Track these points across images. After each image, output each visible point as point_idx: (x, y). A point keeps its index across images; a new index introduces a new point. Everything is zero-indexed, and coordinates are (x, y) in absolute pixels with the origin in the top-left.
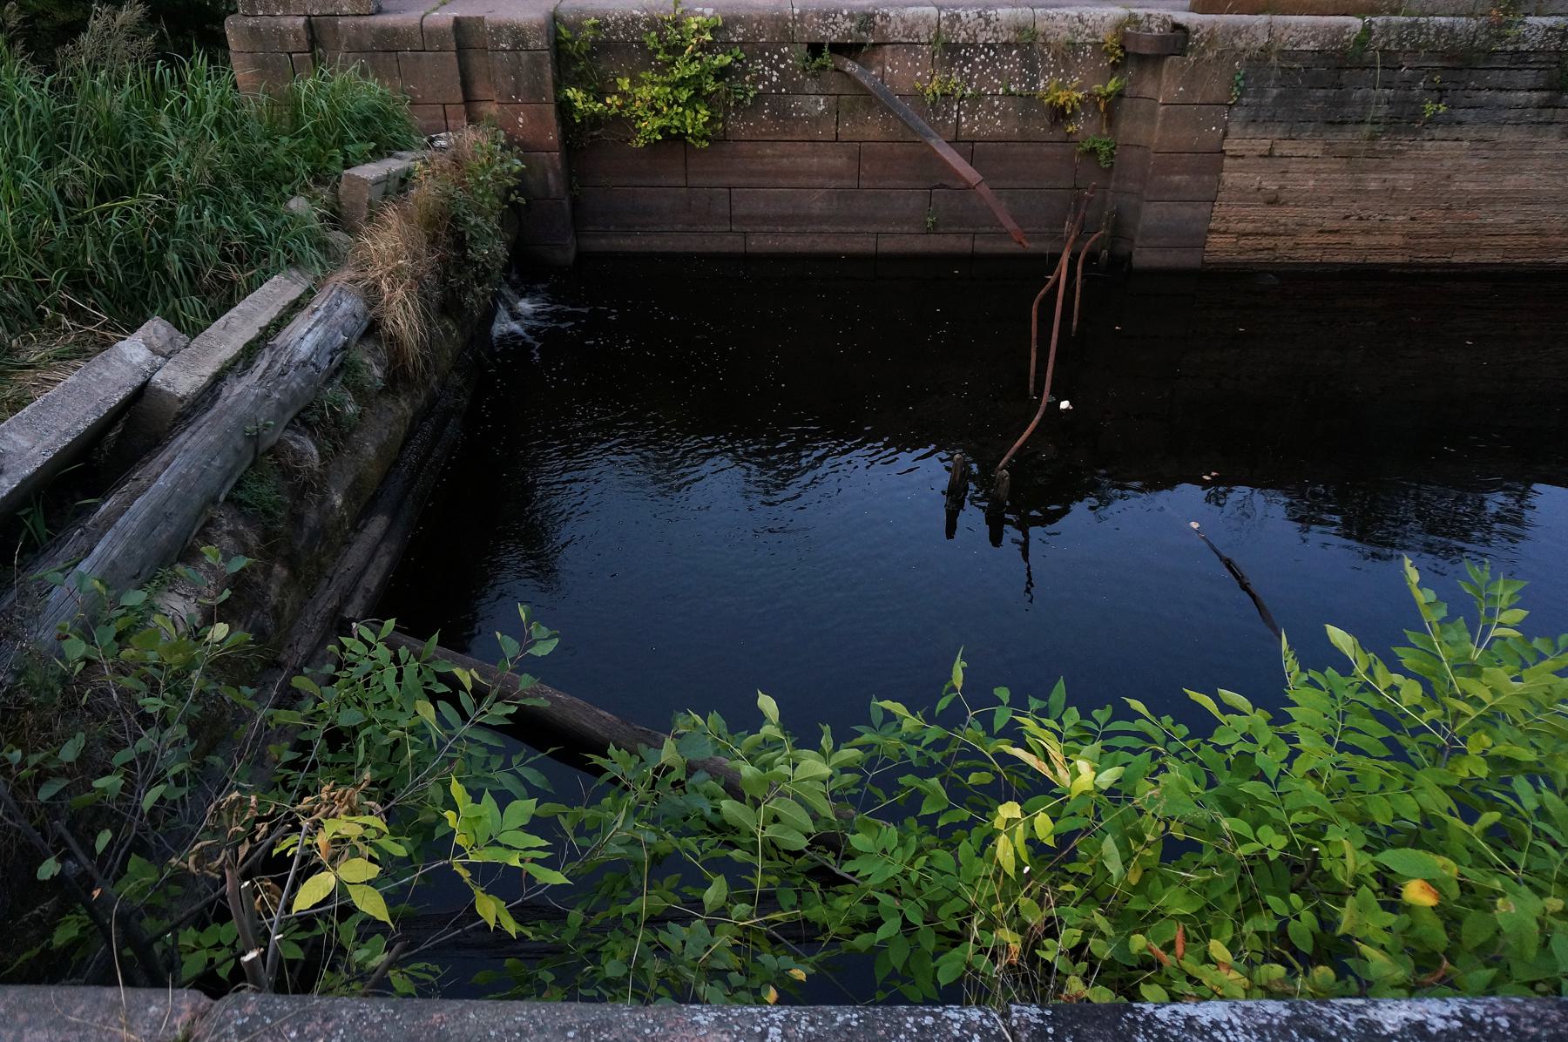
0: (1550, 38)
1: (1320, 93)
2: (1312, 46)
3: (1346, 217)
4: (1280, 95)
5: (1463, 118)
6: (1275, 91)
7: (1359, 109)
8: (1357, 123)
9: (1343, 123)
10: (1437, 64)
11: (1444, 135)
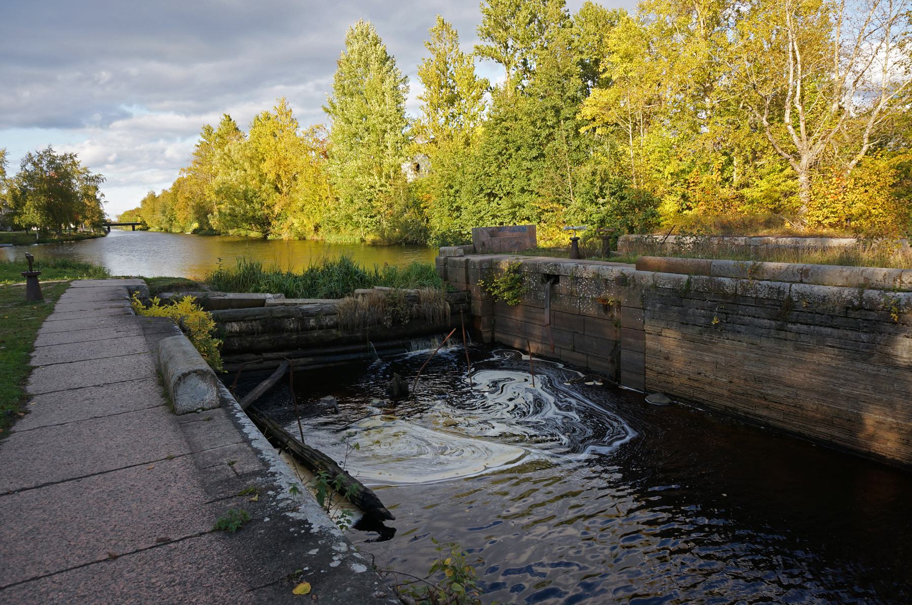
0: (772, 292)
1: (676, 308)
2: (669, 286)
3: (699, 374)
4: (661, 308)
5: (739, 330)
6: (659, 305)
7: (692, 318)
8: (693, 325)
9: (687, 324)
10: (721, 300)
11: (733, 337)
